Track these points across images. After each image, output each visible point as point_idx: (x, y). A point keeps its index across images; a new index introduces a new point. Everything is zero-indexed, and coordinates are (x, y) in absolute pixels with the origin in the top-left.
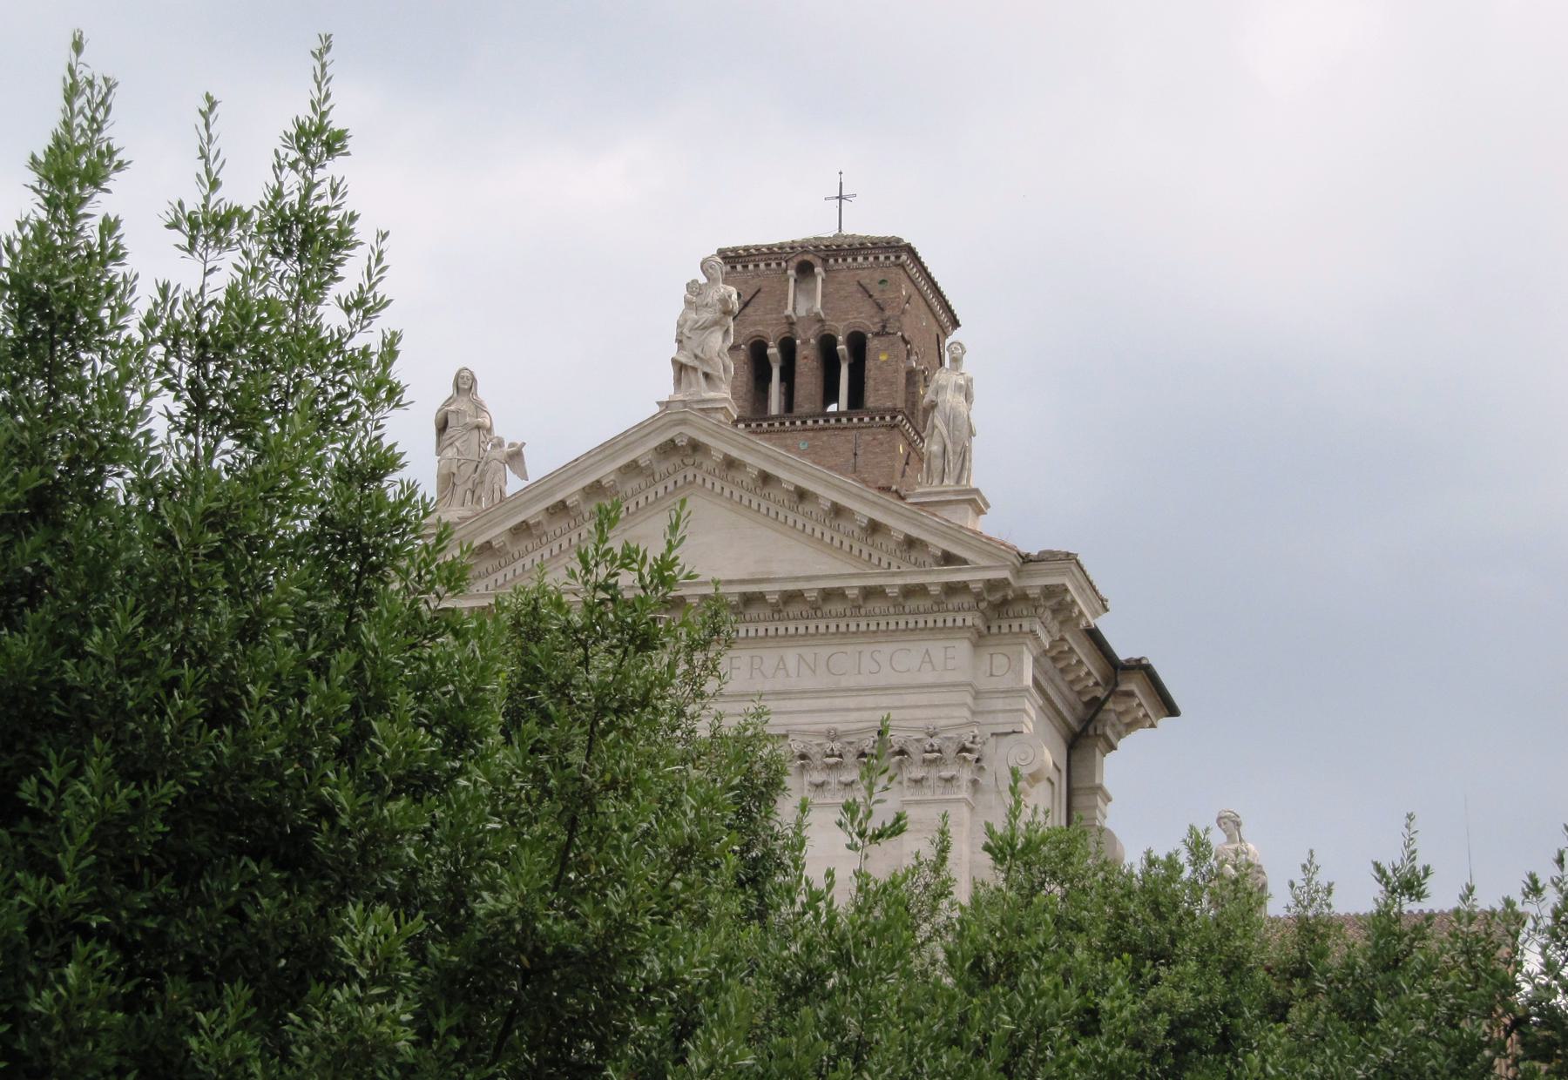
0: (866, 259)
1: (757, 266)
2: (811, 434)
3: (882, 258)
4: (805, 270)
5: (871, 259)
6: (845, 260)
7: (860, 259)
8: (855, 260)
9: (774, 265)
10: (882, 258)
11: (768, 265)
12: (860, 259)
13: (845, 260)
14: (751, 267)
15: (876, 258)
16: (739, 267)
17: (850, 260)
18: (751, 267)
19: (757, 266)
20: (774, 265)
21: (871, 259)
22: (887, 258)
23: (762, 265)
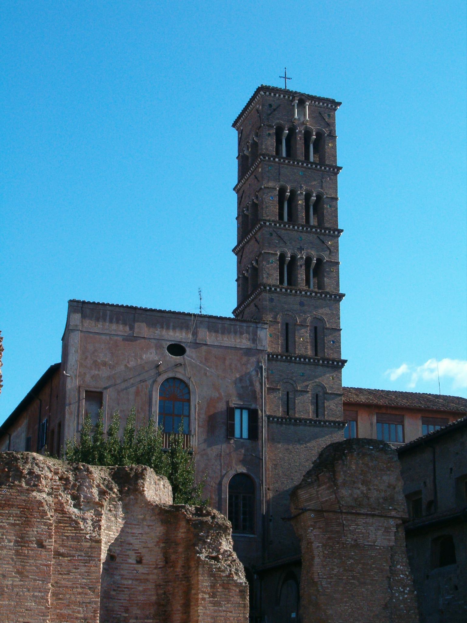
0: (323, 104)
1: (280, 96)
2: (304, 169)
3: (330, 105)
4: (302, 103)
5: (325, 105)
6: (315, 102)
7: (321, 104)
8: (319, 103)
9: (287, 97)
10: (330, 105)
11: (284, 96)
12: (321, 104)
13: (315, 102)
14: (277, 95)
15: (327, 105)
16: (272, 94)
17: (317, 103)
18: (277, 95)
19: (280, 96)
20: (287, 97)
21: (325, 105)
22: (332, 106)
23: (282, 96)
